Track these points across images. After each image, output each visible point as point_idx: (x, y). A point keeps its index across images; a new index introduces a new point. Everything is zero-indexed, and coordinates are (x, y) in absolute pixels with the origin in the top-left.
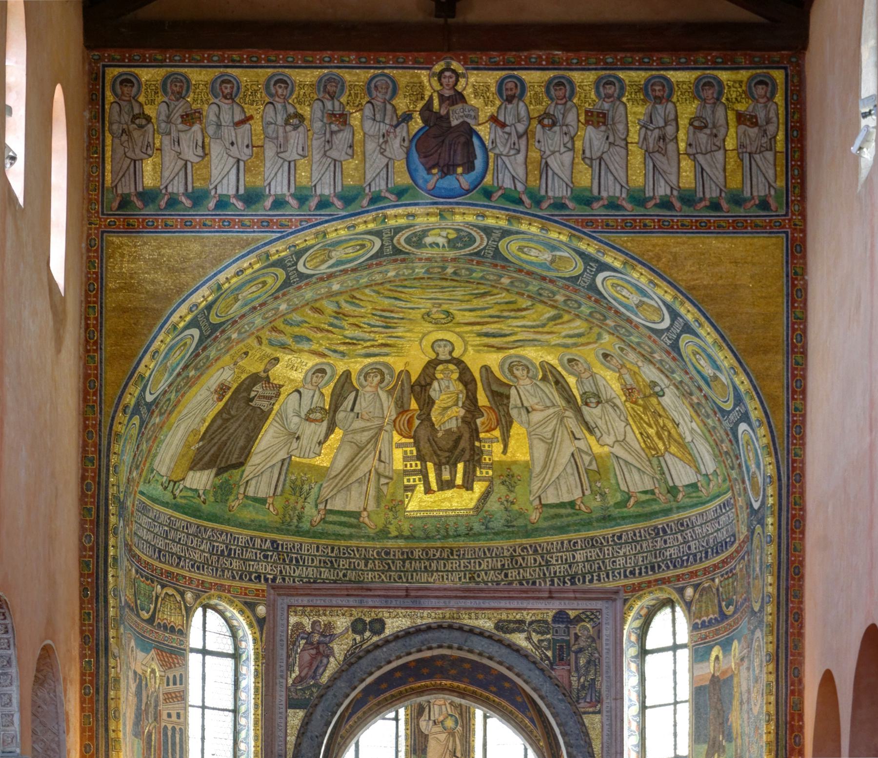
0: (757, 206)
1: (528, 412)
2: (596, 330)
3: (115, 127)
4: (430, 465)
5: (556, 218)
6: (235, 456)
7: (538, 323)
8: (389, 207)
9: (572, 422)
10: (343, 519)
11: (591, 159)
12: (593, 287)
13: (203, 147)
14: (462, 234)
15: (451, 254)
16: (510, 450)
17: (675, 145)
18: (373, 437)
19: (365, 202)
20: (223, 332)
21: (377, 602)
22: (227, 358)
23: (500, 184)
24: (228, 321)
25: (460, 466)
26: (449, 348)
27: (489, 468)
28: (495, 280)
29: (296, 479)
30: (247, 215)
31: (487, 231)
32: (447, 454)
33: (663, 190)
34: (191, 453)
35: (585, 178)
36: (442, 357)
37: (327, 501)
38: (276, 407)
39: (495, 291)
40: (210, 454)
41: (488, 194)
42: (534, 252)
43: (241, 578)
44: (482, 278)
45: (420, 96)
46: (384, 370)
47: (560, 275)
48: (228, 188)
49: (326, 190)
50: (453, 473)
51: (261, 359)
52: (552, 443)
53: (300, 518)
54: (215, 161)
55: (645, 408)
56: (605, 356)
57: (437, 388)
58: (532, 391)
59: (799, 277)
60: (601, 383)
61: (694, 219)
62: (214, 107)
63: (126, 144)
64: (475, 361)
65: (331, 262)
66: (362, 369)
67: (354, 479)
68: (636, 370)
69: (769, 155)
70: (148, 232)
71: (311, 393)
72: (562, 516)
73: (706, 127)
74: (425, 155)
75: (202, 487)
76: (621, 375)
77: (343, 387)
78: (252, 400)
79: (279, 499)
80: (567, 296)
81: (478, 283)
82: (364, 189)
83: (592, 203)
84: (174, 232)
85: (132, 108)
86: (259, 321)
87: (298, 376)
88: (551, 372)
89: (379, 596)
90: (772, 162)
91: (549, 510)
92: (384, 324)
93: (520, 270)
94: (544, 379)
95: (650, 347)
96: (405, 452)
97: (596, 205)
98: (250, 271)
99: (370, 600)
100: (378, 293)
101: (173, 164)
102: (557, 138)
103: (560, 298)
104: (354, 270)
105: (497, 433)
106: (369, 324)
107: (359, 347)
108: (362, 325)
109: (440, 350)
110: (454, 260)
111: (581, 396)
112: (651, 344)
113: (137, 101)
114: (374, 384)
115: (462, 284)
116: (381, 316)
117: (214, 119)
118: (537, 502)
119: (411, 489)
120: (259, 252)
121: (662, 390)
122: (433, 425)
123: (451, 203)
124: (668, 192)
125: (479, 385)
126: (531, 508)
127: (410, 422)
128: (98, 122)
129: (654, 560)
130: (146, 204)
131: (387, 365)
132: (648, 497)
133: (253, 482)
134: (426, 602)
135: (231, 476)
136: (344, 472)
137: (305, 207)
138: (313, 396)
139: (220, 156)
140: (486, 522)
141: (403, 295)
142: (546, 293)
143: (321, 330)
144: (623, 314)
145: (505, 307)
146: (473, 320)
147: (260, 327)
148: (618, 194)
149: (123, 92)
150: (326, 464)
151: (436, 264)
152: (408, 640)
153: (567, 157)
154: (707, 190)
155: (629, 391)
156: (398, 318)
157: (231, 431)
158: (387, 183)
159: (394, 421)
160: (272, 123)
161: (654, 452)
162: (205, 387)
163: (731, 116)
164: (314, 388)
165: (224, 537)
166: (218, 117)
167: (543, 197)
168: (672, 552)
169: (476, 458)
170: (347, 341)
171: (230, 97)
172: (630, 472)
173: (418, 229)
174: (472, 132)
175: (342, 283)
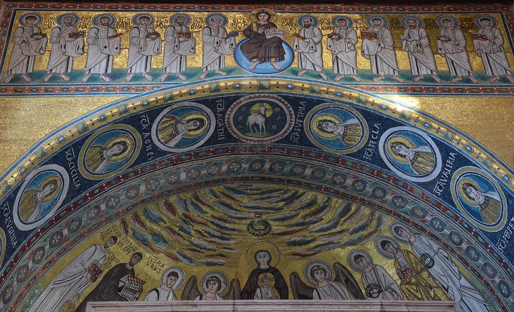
0: (498, 80)
2: (377, 214)
3: (17, 40)
8: (221, 79)
12: (377, 159)
13: (83, 49)
14: (277, 110)
15: (268, 140)
19: (202, 77)
20: (92, 194)
23: (304, 67)
26: (267, 258)
30: (111, 85)
33: (424, 72)
35: (364, 64)
36: (263, 267)
39: (301, 191)
49: (174, 70)
55: (417, 284)
56: (384, 244)
58: (329, 292)
60: (380, 272)
65: (178, 138)
69: (502, 55)
70: (31, 95)
71: (167, 293)
73: (450, 40)
76: (396, 259)
78: (120, 290)
80: (355, 177)
81: (289, 182)
82: (203, 70)
83: (373, 79)
84: (53, 95)
92: (219, 234)
93: (319, 156)
95: (422, 210)
97: (375, 79)
100: (215, 195)
101: (59, 58)
102: (343, 44)
106: (209, 233)
108: (203, 232)
109: (261, 260)
110: (270, 148)
111: (366, 289)
112: (423, 204)
115: (277, 187)
116: (218, 225)
117: (94, 35)
121: (432, 259)
124: (430, 73)
125: (290, 289)
128: (5, 37)
142: (338, 179)
143: (174, 233)
145: (307, 211)
146: (283, 229)
147: (125, 207)
151: (256, 157)
153: (352, 54)
155: (402, 273)
158: (220, 66)
164: (169, 289)
166: (97, 34)
170: (193, 248)
173: (244, 101)
174: (281, 41)
175: (188, 171)
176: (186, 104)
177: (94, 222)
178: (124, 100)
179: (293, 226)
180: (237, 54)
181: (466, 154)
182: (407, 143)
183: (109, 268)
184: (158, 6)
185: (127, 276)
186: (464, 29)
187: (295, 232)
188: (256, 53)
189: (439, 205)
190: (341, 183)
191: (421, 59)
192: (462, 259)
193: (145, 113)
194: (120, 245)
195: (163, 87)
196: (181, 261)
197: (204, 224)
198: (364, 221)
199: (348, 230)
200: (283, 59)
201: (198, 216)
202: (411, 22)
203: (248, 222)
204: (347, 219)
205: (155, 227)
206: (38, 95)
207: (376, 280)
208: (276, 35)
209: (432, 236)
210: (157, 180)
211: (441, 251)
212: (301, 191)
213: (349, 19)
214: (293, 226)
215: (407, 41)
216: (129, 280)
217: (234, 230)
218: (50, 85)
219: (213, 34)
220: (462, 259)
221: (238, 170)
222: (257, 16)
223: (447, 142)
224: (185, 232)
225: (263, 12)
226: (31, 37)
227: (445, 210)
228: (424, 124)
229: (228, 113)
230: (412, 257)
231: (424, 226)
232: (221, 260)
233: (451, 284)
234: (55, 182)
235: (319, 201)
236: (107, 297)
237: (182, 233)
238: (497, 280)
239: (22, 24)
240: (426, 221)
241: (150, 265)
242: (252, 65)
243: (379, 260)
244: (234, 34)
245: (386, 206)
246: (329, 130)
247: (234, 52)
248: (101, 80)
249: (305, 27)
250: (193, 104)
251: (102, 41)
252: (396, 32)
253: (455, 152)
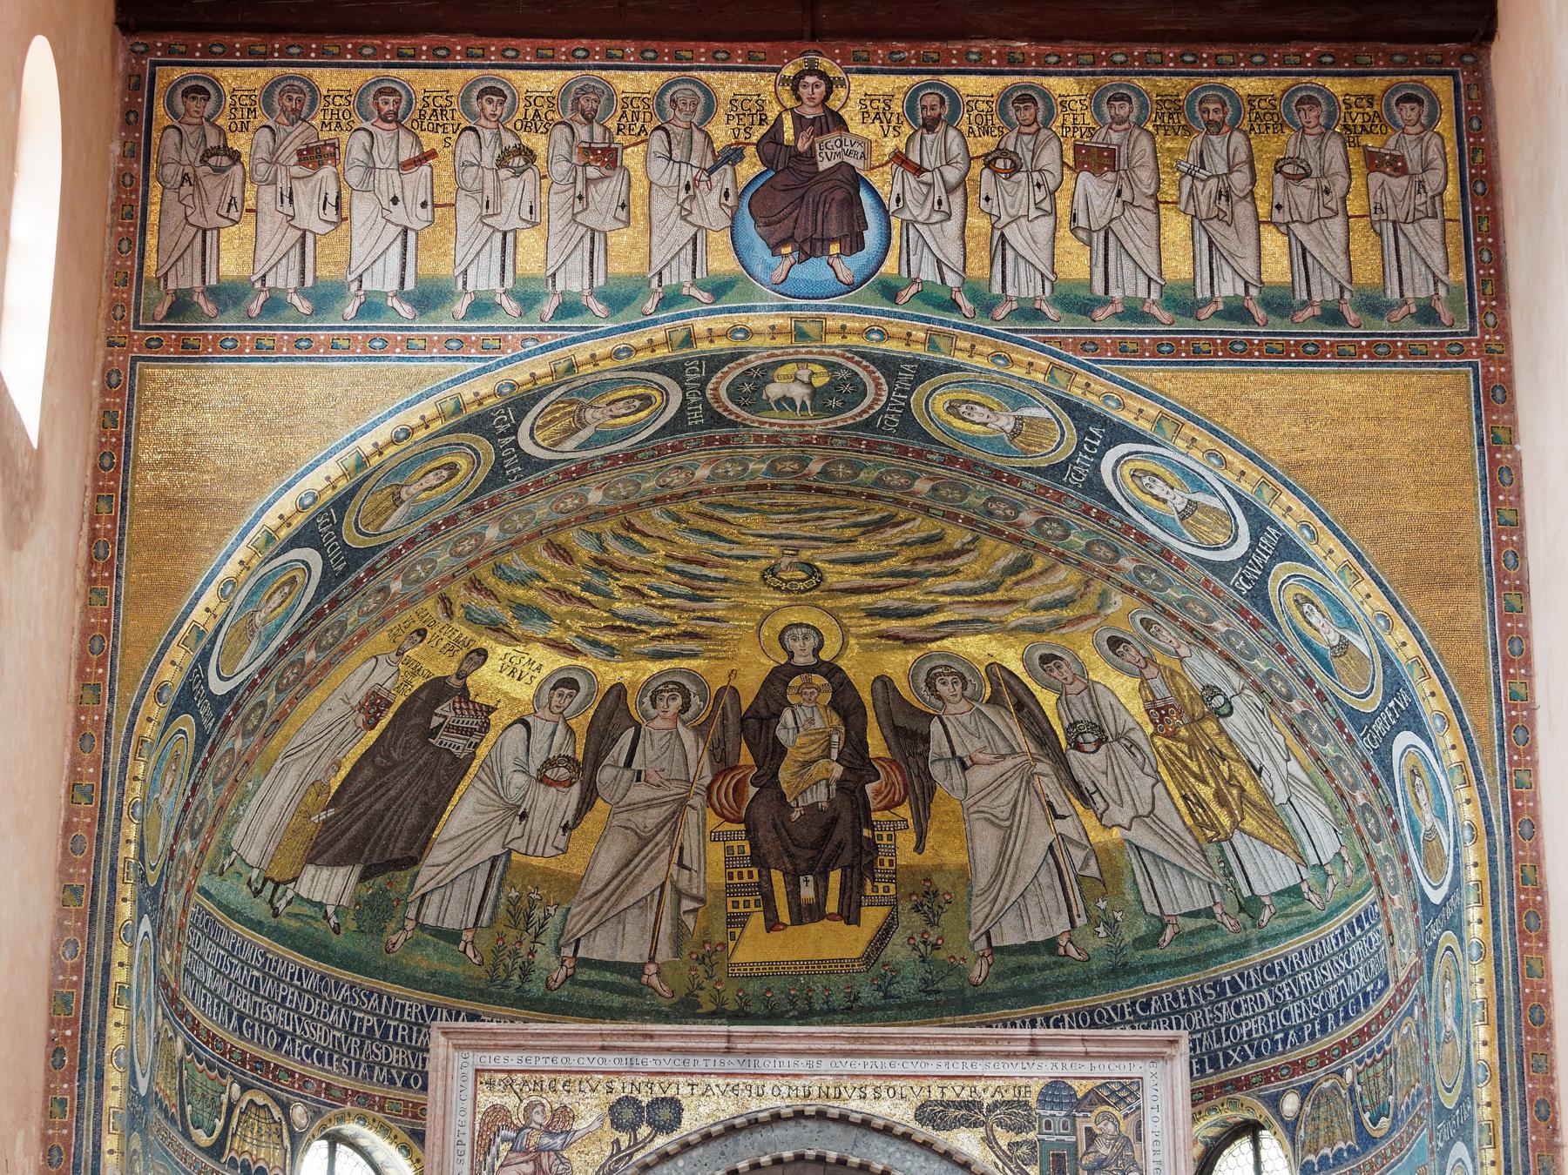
0: (1413, 316)
1: (964, 767)
3: (169, 170)
4: (777, 876)
5: (1023, 336)
6: (400, 844)
7: (983, 582)
8: (697, 314)
9: (1050, 786)
10: (609, 977)
11: (1090, 231)
12: (1094, 486)
14: (842, 374)
15: (817, 426)
16: (932, 838)
17: (1250, 208)
18: (667, 820)
19: (650, 306)
20: (372, 571)
21: (666, 1063)
22: (383, 636)
23: (913, 275)
24: (381, 547)
25: (835, 877)
26: (812, 643)
27: (890, 880)
28: (902, 487)
29: (519, 898)
30: (418, 329)
31: (888, 365)
32: (810, 853)
33: (1229, 287)
34: (310, 827)
35: (1076, 263)
36: (799, 660)
37: (578, 941)
38: (482, 751)
40: (348, 835)
41: (890, 292)
42: (979, 414)
43: (406, 1084)
44: (878, 482)
45: (757, 119)
46: (689, 685)
47: (1028, 463)
48: (383, 279)
49: (574, 282)
50: (821, 890)
51: (450, 650)
52: (1011, 826)
53: (525, 973)
54: (359, 232)
55: (1192, 743)
56: (1114, 643)
57: (791, 723)
58: (972, 727)
59: (1504, 447)
61: (1292, 340)
62: (363, 137)
63: (188, 201)
64: (859, 669)
65: (584, 434)
66: (648, 683)
67: (632, 901)
68: (1176, 665)
69: (1432, 226)
70: (223, 360)
71: (549, 727)
72: (1032, 970)
73: (1307, 175)
74: (766, 221)
75: (332, 900)
76: (1144, 680)
77: (610, 717)
78: (434, 733)
79: (486, 934)
81: (871, 497)
84: (276, 360)
85: (205, 136)
86: (443, 558)
87: (523, 692)
88: (1007, 683)
89: (669, 1050)
90: (1438, 237)
91: (1007, 958)
93: (951, 460)
94: (995, 700)
95: (1205, 607)
96: (728, 850)
97: (1100, 314)
98: (422, 434)
99: (650, 1058)
100: (679, 520)
101: (278, 236)
102: (1022, 192)
103: (1028, 518)
104: (629, 458)
105: (904, 811)
106: (659, 590)
107: (642, 637)
108: (646, 591)
109: (796, 646)
110: (823, 439)
111: (1066, 731)
112: (1207, 598)
113: (213, 125)
115: (840, 502)
116: (682, 573)
117: (362, 156)
118: (983, 943)
119: (737, 921)
120: (441, 395)
121: (1227, 701)
122: (783, 796)
123: (817, 308)
124: (1241, 291)
125: (871, 714)
126: (970, 957)
127: (739, 789)
128: (138, 162)
129: (1217, 1046)
130: (222, 309)
131: (691, 674)
132: (1200, 923)
133: (436, 898)
134: (768, 1064)
135: (390, 883)
136: (612, 887)
137: (534, 315)
138: (553, 733)
139: (371, 222)
140: (885, 984)
141: (724, 528)
142: (1000, 509)
143: (569, 597)
144: (1153, 539)
145: (920, 551)
146: (858, 581)
147: (449, 573)
148: (1142, 294)
149: (187, 110)
150: (578, 871)
151: (788, 452)
152: (730, 1142)
154: (1315, 288)
155: (1159, 712)
156: (716, 579)
157: (392, 793)
158: (694, 272)
159: (709, 789)
160: (472, 165)
161: (1210, 834)
162: (339, 694)
163: (1355, 156)
164: (555, 717)
165: (374, 1002)
166: (370, 154)
167: (998, 297)
168: (1252, 1027)
169: (865, 861)
171: (395, 119)
172: (1164, 876)
173: (754, 361)
175: (605, 487)
176: (608, 376)
177: (374, 616)
178: (455, 382)
179: (880, 576)
180: (739, 228)
181: (1301, 538)
182: (1168, 476)
184: (527, 45)
186: (1350, 135)
187: (888, 588)
188: (789, 223)
189: (1243, 613)
190: (1006, 517)
191: (1224, 242)
192: (1292, 726)
193: (505, 407)
195: (550, 339)
197: (647, 573)
198: (1067, 592)
199: (1026, 602)
200: (860, 245)
201: (632, 558)
202: (1212, 107)
203: (764, 563)
204: (1023, 580)
205: (520, 592)
206: (240, 359)
207: (1092, 713)
208: (846, 159)
209: (1229, 660)
210: (529, 512)
211: (1247, 692)
212: (902, 515)
213: (1046, 95)
214: (880, 576)
215: (1194, 177)
217: (725, 580)
218: (266, 328)
219: (677, 154)
220: (1292, 726)
221: (737, 474)
222: (795, 83)
223: (1263, 501)
224: (596, 592)
225: (811, 71)
226: (204, 162)
227: (1256, 625)
228: (1211, 454)
229: (714, 380)
230: (1182, 685)
231: (1210, 637)
232: (691, 645)
233: (1267, 763)
234: (293, 580)
235: (949, 539)
237: (586, 595)
238: (1361, 801)
239: (175, 115)
240: (1214, 630)
242: (781, 267)
243: (1103, 674)
244: (733, 155)
245: (1120, 578)
246: (976, 418)
247: (733, 219)
248: (391, 313)
249: (924, 125)
250: (624, 374)
251: (383, 177)
252: (1168, 145)
253: (1278, 528)
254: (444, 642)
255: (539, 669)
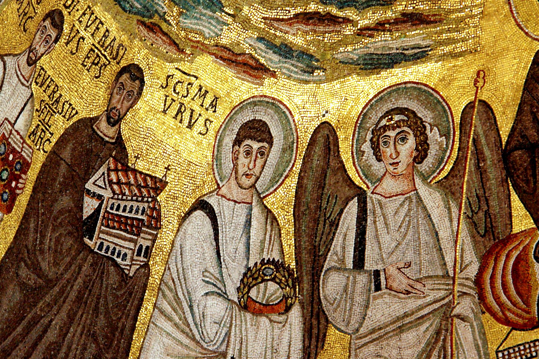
66: (364, 116)
71: (241, 210)
107: (348, 30)
114: (401, 168)
138: (248, 223)
157: (51, 336)
159: (478, 281)
183: (48, 147)
185: (103, 169)
194: (73, 45)
196: (273, 75)
216: (111, 182)
236: (56, 264)
241: (176, 107)
254: (86, 46)
255: (213, 105)
